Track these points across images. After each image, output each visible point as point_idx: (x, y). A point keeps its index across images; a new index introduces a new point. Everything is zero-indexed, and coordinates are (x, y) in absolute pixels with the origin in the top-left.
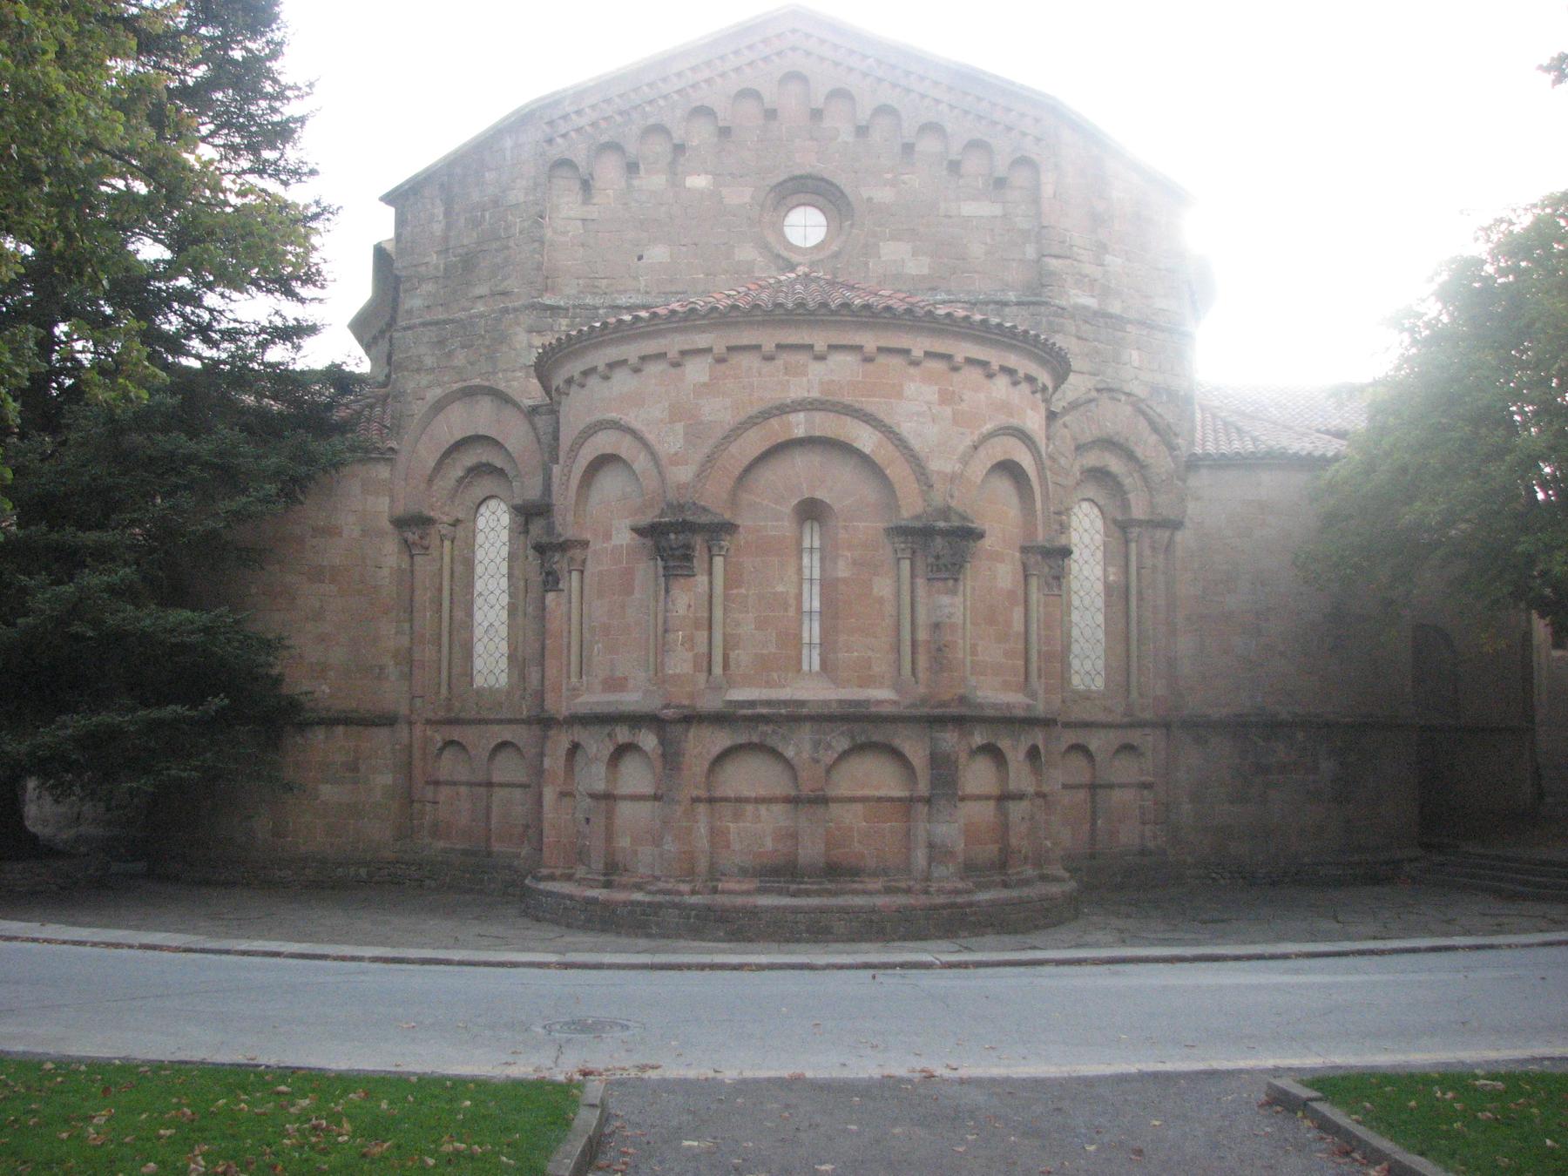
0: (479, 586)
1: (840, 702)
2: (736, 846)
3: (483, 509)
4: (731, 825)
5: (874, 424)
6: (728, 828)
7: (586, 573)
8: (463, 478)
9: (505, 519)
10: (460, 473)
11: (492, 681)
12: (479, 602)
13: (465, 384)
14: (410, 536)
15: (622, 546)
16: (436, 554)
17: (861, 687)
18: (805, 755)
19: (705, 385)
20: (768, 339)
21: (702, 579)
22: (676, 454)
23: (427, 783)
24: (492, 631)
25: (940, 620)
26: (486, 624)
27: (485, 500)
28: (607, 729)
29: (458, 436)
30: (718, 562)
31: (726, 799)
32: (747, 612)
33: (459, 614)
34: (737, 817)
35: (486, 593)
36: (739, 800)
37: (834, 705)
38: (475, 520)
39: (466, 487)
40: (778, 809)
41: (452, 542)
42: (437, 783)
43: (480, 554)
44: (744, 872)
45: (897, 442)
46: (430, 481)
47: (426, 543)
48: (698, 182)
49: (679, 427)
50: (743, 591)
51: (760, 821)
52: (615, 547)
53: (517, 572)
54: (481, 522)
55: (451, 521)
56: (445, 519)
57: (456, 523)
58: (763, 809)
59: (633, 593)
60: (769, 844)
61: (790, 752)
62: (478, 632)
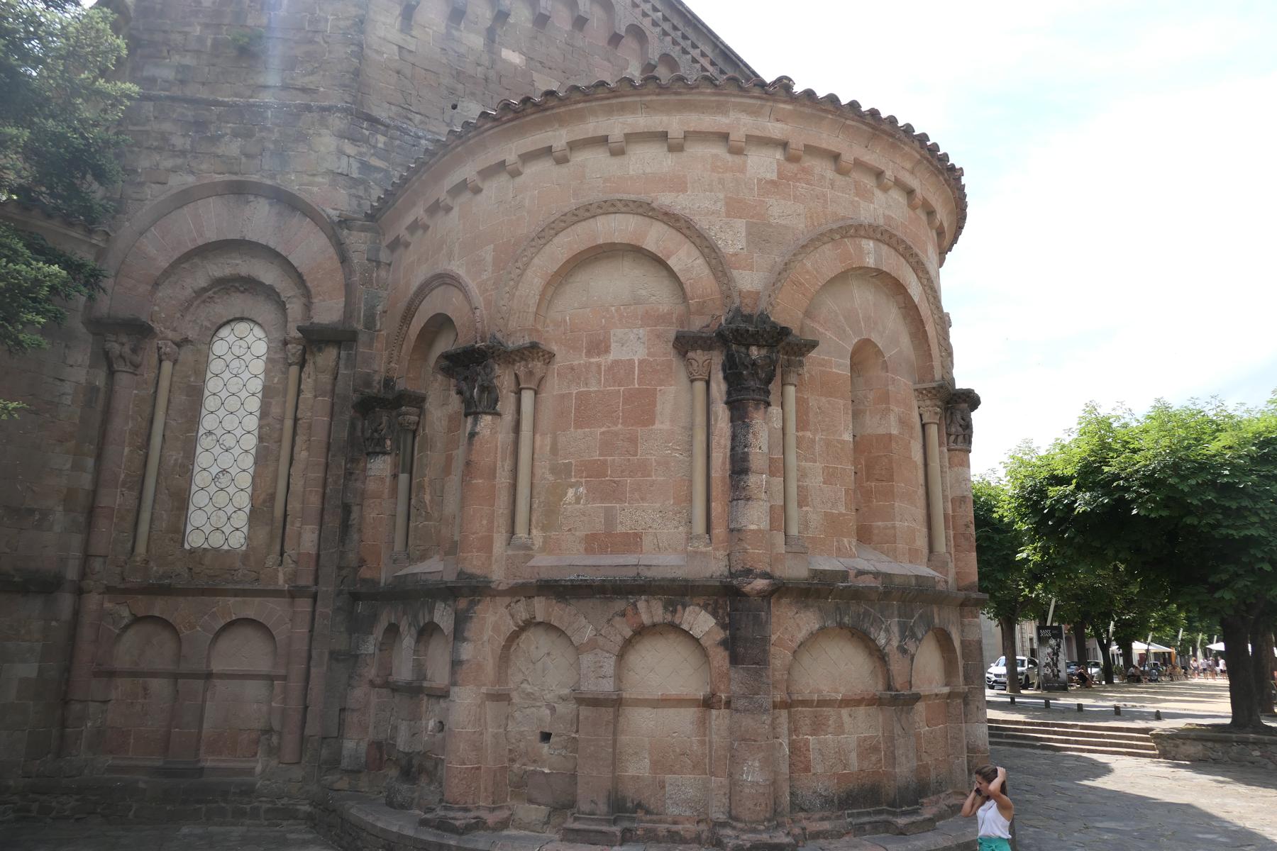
0: (208, 422)
1: (917, 577)
2: (819, 769)
3: (224, 332)
4: (809, 737)
5: (920, 275)
6: (807, 742)
7: (543, 395)
8: (205, 290)
9: (261, 348)
10: (202, 282)
11: (216, 541)
12: (205, 442)
13: (234, 178)
14: (115, 348)
15: (631, 362)
16: (149, 375)
17: (910, 562)
18: (895, 643)
19: (772, 182)
20: (852, 150)
21: (775, 410)
22: (736, 255)
23: (97, 674)
24: (224, 480)
25: (965, 493)
26: (215, 470)
27: (228, 322)
28: (620, 605)
29: (212, 236)
30: (791, 390)
31: (805, 703)
32: (815, 462)
33: (175, 456)
34: (818, 727)
35: (219, 432)
36: (823, 703)
37: (913, 582)
38: (210, 343)
39: (204, 302)
40: (861, 711)
41: (174, 364)
42: (112, 674)
43: (212, 385)
44: (827, 802)
45: (932, 300)
46: (156, 285)
47: (137, 359)
48: (512, 57)
49: (740, 225)
50: (808, 434)
51: (843, 733)
52: (616, 362)
53: (275, 410)
54: (219, 347)
55: (178, 338)
56: (170, 334)
57: (183, 342)
58: (845, 712)
59: (652, 421)
60: (854, 763)
61: (882, 641)
62: (200, 479)
